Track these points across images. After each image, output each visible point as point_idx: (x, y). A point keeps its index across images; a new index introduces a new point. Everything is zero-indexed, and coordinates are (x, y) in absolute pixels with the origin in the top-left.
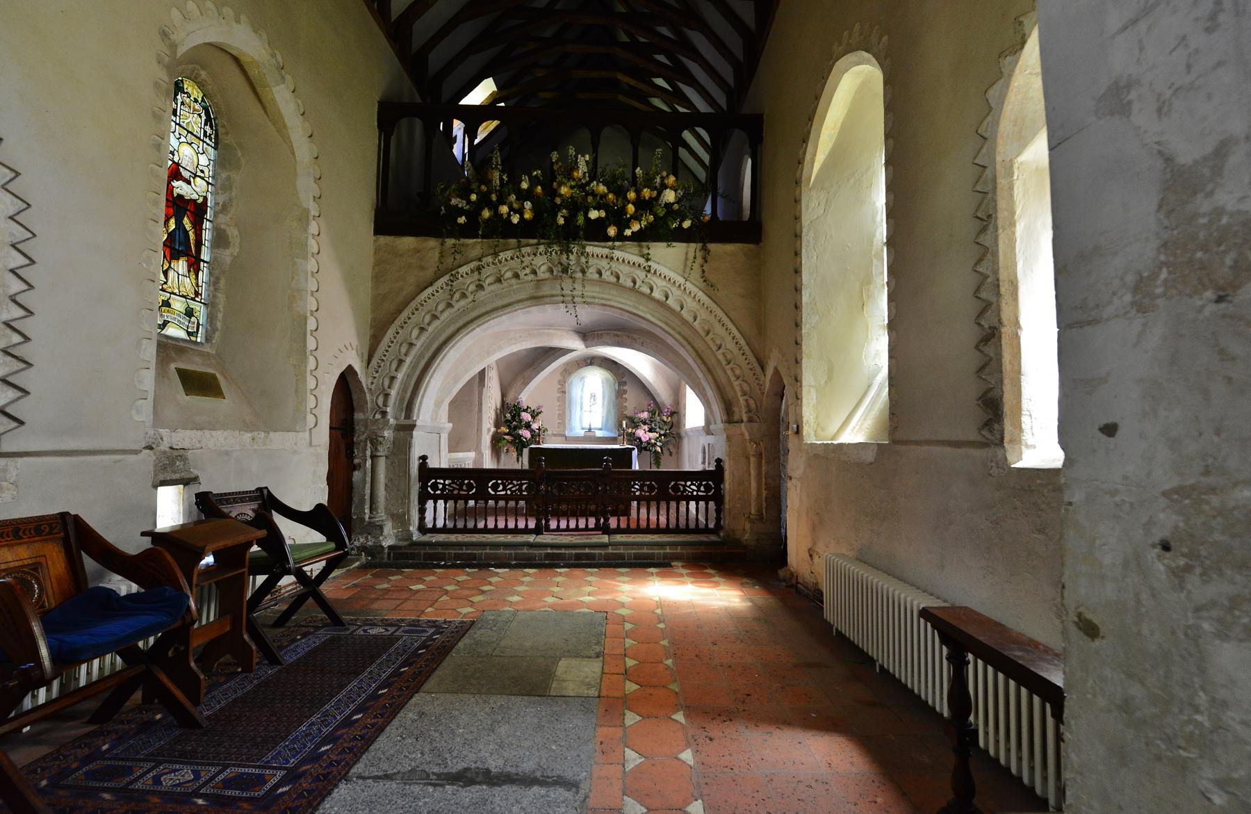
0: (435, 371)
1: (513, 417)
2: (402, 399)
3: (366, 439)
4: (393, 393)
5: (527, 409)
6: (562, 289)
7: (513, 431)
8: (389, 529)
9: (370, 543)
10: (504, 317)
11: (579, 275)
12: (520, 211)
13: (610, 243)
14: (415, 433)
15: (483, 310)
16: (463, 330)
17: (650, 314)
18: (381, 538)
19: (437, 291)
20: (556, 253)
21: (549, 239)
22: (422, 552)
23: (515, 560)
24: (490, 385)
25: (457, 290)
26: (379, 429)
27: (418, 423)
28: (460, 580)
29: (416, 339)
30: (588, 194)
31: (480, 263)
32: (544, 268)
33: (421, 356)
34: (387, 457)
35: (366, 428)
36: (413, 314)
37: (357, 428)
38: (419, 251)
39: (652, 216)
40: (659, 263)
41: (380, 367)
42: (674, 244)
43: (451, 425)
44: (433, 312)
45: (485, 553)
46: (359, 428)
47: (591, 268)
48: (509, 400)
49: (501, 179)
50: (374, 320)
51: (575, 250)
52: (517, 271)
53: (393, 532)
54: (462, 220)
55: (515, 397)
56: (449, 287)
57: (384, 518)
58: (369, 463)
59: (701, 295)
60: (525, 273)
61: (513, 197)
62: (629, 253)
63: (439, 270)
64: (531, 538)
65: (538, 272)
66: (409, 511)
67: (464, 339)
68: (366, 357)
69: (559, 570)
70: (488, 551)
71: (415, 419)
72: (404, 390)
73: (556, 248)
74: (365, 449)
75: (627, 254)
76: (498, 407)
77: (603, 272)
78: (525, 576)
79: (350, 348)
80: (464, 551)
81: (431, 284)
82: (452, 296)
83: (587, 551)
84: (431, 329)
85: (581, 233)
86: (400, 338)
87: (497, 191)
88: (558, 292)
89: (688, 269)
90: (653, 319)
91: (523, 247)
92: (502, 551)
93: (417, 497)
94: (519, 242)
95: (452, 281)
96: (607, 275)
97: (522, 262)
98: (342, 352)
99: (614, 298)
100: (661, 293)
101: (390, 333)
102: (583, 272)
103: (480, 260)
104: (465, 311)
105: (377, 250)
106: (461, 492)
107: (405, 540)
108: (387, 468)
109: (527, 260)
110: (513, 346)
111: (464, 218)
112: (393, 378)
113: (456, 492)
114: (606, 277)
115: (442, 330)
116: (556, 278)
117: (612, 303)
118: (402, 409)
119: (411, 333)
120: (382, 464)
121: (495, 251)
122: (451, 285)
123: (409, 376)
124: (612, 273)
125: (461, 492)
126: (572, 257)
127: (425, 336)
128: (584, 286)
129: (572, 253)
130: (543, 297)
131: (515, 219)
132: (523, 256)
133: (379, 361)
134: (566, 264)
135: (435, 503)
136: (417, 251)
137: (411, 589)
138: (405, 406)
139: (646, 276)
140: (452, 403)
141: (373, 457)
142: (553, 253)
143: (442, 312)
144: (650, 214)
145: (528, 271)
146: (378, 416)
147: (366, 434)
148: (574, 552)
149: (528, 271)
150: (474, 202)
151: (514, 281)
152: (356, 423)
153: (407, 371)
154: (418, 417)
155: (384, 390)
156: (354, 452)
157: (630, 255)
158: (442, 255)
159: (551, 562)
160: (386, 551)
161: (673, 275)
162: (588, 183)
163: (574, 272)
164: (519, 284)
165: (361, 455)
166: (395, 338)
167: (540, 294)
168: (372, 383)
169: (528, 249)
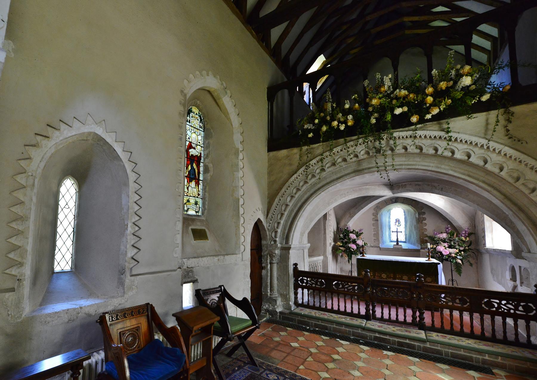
0: (299, 218)
1: (345, 236)
3: (267, 254)
4: (279, 231)
5: (353, 232)
6: (377, 163)
7: (345, 245)
8: (279, 302)
9: (271, 309)
10: (338, 185)
11: (389, 152)
12: (345, 122)
13: (413, 127)
14: (290, 251)
15: (324, 183)
16: (314, 195)
17: (452, 170)
18: (276, 307)
19: (299, 176)
20: (371, 142)
21: (366, 134)
23: (353, 335)
24: (330, 219)
25: (310, 174)
26: (273, 249)
27: (292, 246)
28: (319, 345)
29: (289, 202)
30: (392, 99)
31: (322, 157)
32: (362, 152)
33: (292, 210)
34: (277, 264)
35: (267, 249)
36: (287, 189)
37: (263, 248)
38: (289, 156)
39: (450, 100)
40: (459, 133)
41: (272, 218)
42: (474, 115)
43: (309, 245)
44: (298, 187)
45: (333, 327)
46: (264, 248)
47: (398, 146)
48: (342, 225)
49: (332, 107)
50: (268, 194)
51: (385, 137)
52: (345, 157)
53: (282, 304)
54: (311, 135)
55: (345, 225)
56: (305, 173)
57: (277, 296)
59: (510, 151)
60: (350, 158)
61: (340, 115)
62: (430, 130)
63: (300, 164)
64: (363, 323)
65: (359, 155)
66: (289, 294)
67: (314, 200)
68: (266, 213)
69: (385, 352)
70: (335, 326)
71: (290, 244)
72: (285, 229)
73: (371, 138)
74: (267, 260)
75: (428, 131)
76: (335, 231)
77: (408, 147)
78: (361, 352)
79: (258, 210)
80: (320, 323)
81: (296, 173)
82: (307, 177)
83: (407, 341)
84: (297, 196)
85: (389, 125)
87: (330, 114)
88: (374, 165)
89: (490, 132)
90: (456, 174)
91: (348, 142)
92: (343, 328)
93: (293, 286)
94: (345, 140)
95: (307, 169)
96: (412, 149)
97: (348, 151)
98: (255, 213)
99: (418, 163)
100: (463, 154)
101: (277, 200)
102: (392, 150)
103: (322, 155)
104: (315, 184)
106: (317, 286)
107: (288, 309)
108: (278, 269)
109: (351, 150)
110: (343, 198)
111: (312, 134)
112: (279, 223)
113: (314, 285)
114: (411, 150)
115: (302, 196)
116: (372, 157)
117: (417, 167)
118: (284, 239)
119: (287, 199)
120: (275, 267)
121: (330, 148)
122: (306, 172)
123: (286, 221)
124: (416, 147)
125: (317, 286)
126: (382, 142)
127: (294, 200)
128: (393, 159)
129: (383, 139)
130: (363, 170)
131: (342, 127)
132: (349, 148)
133: (272, 215)
134: (379, 147)
135: (303, 290)
136: (288, 156)
137: (291, 346)
138: (285, 237)
139: (448, 144)
140: (309, 234)
141: (271, 263)
142: (369, 142)
143: (302, 186)
144: (448, 99)
145: (352, 156)
146: (272, 243)
147: (267, 252)
148: (397, 340)
149: (352, 156)
150: (317, 124)
151: (343, 163)
152: (262, 246)
153: (285, 219)
154: (292, 243)
155: (275, 229)
156: (262, 261)
157: (431, 131)
158: (301, 156)
159: (379, 343)
160: (278, 314)
161: (474, 139)
162: (392, 92)
163: (385, 151)
164: (346, 164)
165: (265, 262)
166: (279, 202)
167: (361, 168)
168: (269, 226)
169: (352, 143)
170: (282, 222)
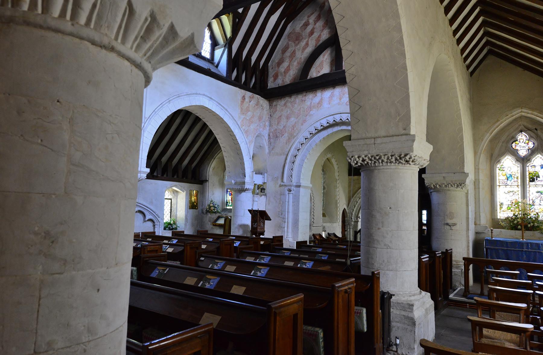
2: (355, 215)
4: (353, 213)
46: (346, 221)
58: (349, 230)
72: (356, 213)
112: (353, 210)
123: (357, 209)
146: (350, 219)
170: (355, 209)
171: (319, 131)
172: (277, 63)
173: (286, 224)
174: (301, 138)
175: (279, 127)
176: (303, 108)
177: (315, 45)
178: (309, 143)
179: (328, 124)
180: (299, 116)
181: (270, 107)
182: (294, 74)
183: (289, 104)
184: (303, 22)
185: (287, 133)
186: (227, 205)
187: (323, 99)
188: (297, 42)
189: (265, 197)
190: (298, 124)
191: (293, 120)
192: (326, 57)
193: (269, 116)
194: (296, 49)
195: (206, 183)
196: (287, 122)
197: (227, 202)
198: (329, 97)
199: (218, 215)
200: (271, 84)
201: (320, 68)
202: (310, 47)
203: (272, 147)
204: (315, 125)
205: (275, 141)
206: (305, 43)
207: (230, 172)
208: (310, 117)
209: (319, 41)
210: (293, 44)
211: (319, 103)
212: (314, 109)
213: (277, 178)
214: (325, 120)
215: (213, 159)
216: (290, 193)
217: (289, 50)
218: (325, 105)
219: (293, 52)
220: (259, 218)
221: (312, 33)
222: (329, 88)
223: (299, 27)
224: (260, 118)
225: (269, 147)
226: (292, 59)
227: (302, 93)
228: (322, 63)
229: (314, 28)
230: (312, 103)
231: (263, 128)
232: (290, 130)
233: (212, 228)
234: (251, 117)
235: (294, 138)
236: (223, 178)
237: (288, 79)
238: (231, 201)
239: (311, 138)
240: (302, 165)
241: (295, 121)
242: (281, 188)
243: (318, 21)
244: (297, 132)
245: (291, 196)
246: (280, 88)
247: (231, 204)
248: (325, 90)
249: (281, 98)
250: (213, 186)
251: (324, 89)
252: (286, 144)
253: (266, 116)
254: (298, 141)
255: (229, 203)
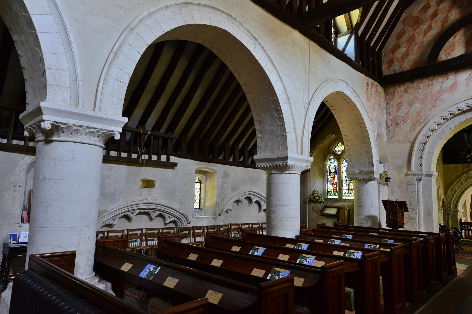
3: (446, 214)
22: (465, 243)
82: (467, 179)
86: (453, 190)
105: (444, 169)
112: (451, 200)
138: (454, 206)
146: (448, 209)
147: (445, 213)
168: (446, 201)
171: (455, 116)
172: (391, 49)
173: (417, 215)
174: (431, 125)
175: (399, 114)
176: (430, 92)
177: (440, 28)
178: (440, 129)
179: (468, 108)
180: (425, 101)
181: (385, 94)
182: (415, 59)
183: (411, 90)
184: (422, 5)
185: (410, 119)
186: (328, 194)
187: (457, 82)
188: (416, 26)
189: (387, 187)
190: (425, 110)
191: (417, 106)
192: (458, 37)
193: (385, 104)
194: (415, 34)
195: (307, 173)
196: (410, 108)
197: (328, 192)
198: (466, 79)
199: (323, 205)
200: (386, 71)
201: (450, 50)
202: (435, 30)
203: (391, 135)
204: (450, 110)
205: (395, 128)
206: (426, 26)
207: (352, 162)
208: (440, 102)
209: (447, 22)
210: (411, 29)
211: (452, 86)
212: (445, 93)
213: (401, 167)
214: (464, 103)
215: (314, 150)
216: (420, 182)
217: (406, 35)
218: (462, 87)
219: (411, 37)
220: (399, 209)
221: (435, 15)
222: (465, 69)
223: (418, 11)
224: (379, 106)
225: (387, 135)
226: (411, 44)
227: (428, 78)
228: (453, 44)
229: (438, 10)
230: (443, 87)
231: (382, 116)
232: (415, 116)
233: (317, 218)
234: (373, 104)
235: (420, 124)
236: (323, 168)
237: (407, 65)
238: (333, 191)
239: (445, 123)
240: (433, 153)
241: (420, 107)
242: (408, 177)
243: (442, 2)
244: (425, 119)
245: (421, 185)
246: (396, 75)
247: (333, 194)
248: (460, 73)
249: (399, 85)
250: (314, 176)
251: (459, 71)
252: (410, 131)
253: (383, 104)
254: (427, 127)
255: (330, 193)
